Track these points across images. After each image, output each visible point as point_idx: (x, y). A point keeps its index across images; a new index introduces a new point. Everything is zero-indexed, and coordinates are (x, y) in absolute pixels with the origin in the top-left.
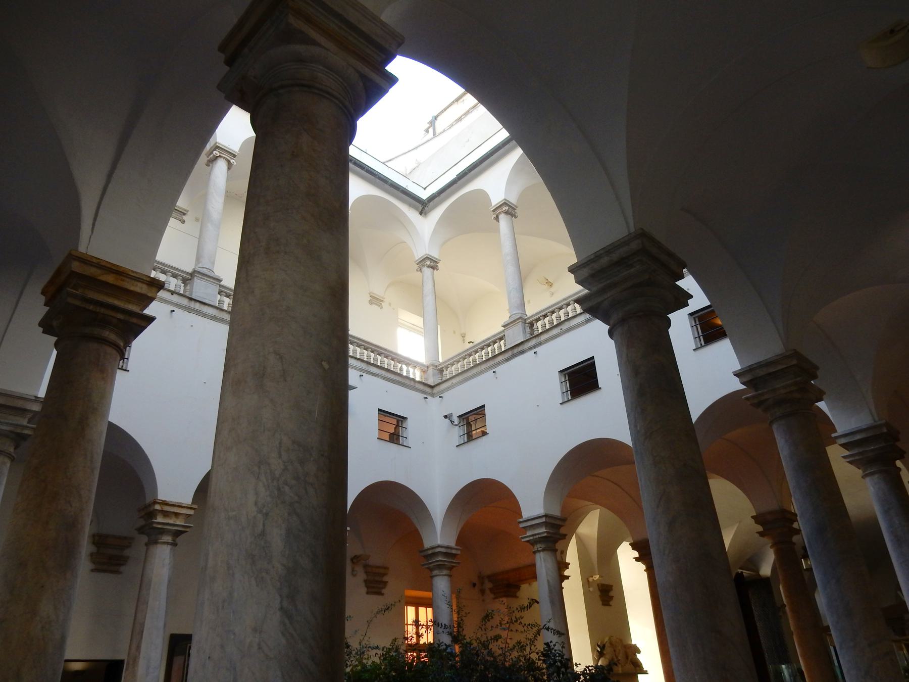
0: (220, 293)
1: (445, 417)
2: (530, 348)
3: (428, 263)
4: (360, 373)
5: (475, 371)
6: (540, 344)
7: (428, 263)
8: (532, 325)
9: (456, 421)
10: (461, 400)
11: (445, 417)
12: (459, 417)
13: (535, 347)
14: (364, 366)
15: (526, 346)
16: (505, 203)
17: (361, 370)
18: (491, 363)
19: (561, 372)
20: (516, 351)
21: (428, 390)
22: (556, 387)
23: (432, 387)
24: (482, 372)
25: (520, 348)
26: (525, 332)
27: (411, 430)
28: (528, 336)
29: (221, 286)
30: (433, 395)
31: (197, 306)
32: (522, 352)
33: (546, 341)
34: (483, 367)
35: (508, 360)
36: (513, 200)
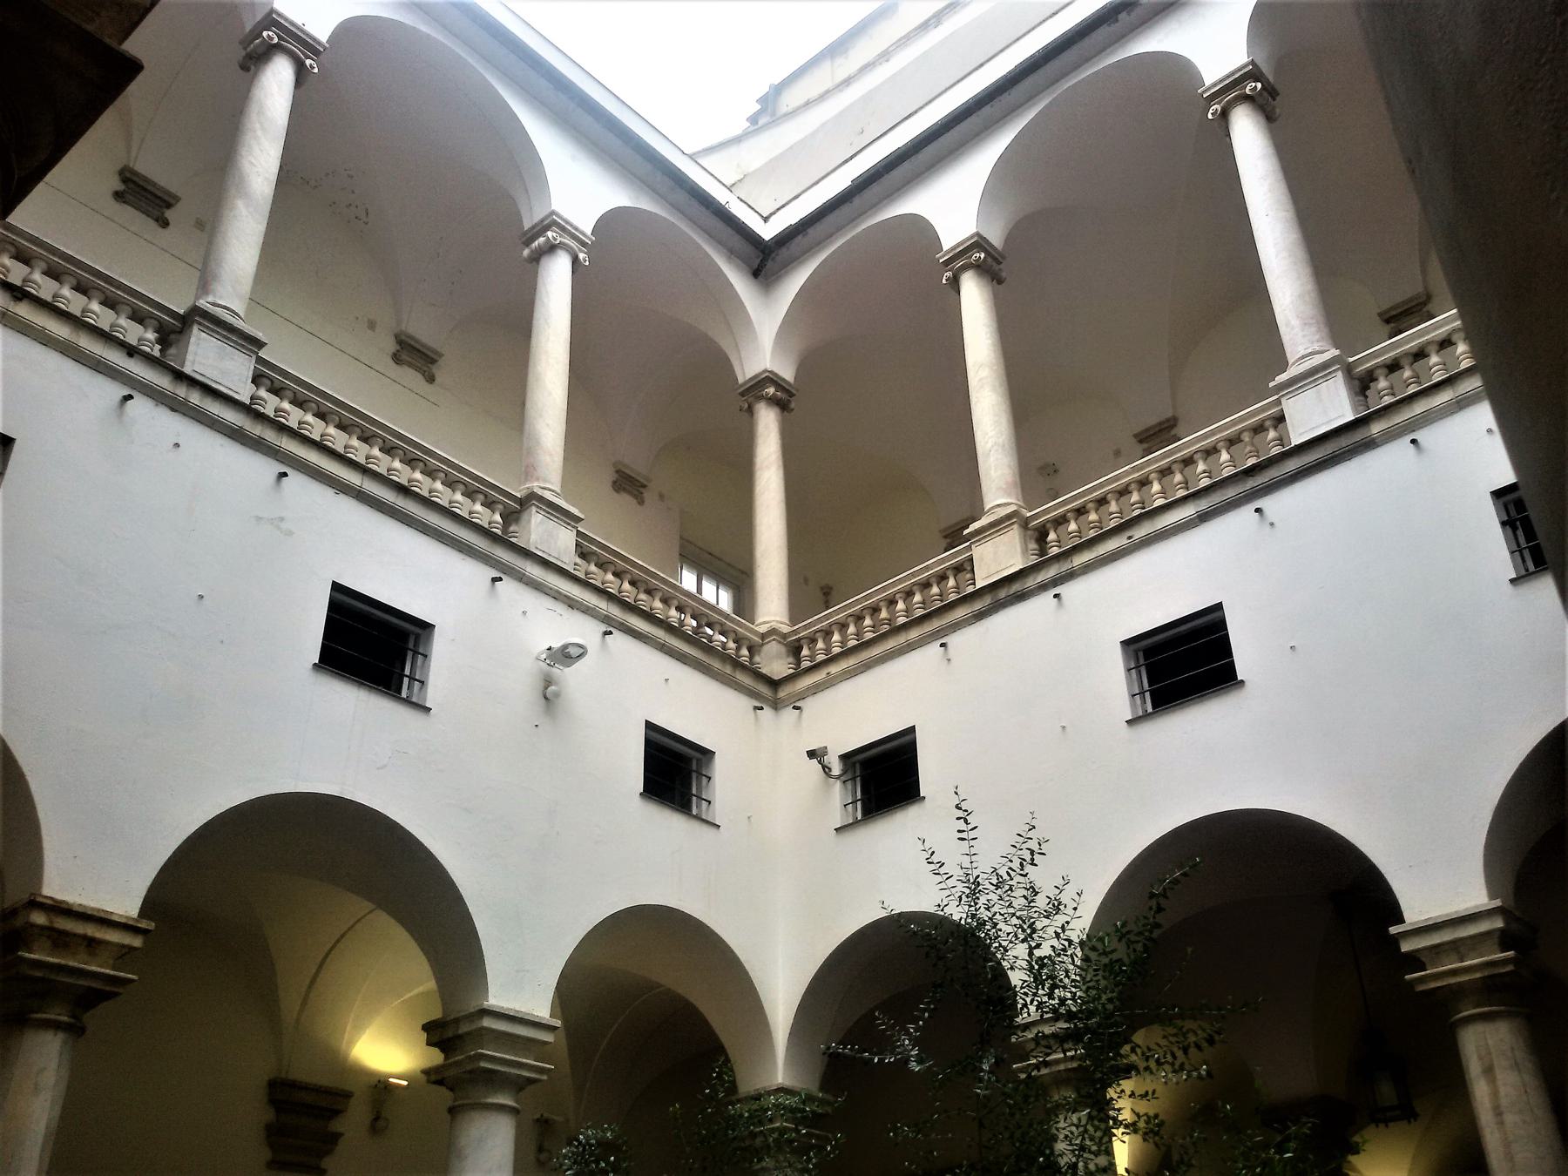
0: (257, 379)
1: (812, 754)
2: (1043, 587)
3: (771, 390)
4: (604, 628)
5: (891, 644)
6: (1071, 576)
7: (771, 390)
8: (1041, 536)
9: (837, 769)
10: (857, 712)
11: (812, 754)
12: (845, 758)
13: (1056, 582)
14: (615, 611)
15: (1031, 582)
16: (979, 243)
17: (606, 620)
18: (936, 624)
19: (1126, 644)
20: (1002, 594)
21: (764, 690)
22: (1114, 683)
23: (775, 684)
24: (910, 647)
25: (1016, 587)
26: (1025, 551)
27: (725, 785)
28: (1033, 560)
29: (260, 360)
30: (776, 705)
31: (195, 398)
32: (1022, 597)
33: (1088, 568)
34: (914, 634)
35: (980, 616)
36: (996, 238)
